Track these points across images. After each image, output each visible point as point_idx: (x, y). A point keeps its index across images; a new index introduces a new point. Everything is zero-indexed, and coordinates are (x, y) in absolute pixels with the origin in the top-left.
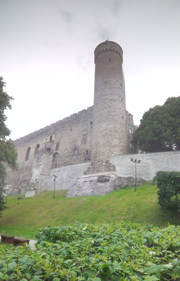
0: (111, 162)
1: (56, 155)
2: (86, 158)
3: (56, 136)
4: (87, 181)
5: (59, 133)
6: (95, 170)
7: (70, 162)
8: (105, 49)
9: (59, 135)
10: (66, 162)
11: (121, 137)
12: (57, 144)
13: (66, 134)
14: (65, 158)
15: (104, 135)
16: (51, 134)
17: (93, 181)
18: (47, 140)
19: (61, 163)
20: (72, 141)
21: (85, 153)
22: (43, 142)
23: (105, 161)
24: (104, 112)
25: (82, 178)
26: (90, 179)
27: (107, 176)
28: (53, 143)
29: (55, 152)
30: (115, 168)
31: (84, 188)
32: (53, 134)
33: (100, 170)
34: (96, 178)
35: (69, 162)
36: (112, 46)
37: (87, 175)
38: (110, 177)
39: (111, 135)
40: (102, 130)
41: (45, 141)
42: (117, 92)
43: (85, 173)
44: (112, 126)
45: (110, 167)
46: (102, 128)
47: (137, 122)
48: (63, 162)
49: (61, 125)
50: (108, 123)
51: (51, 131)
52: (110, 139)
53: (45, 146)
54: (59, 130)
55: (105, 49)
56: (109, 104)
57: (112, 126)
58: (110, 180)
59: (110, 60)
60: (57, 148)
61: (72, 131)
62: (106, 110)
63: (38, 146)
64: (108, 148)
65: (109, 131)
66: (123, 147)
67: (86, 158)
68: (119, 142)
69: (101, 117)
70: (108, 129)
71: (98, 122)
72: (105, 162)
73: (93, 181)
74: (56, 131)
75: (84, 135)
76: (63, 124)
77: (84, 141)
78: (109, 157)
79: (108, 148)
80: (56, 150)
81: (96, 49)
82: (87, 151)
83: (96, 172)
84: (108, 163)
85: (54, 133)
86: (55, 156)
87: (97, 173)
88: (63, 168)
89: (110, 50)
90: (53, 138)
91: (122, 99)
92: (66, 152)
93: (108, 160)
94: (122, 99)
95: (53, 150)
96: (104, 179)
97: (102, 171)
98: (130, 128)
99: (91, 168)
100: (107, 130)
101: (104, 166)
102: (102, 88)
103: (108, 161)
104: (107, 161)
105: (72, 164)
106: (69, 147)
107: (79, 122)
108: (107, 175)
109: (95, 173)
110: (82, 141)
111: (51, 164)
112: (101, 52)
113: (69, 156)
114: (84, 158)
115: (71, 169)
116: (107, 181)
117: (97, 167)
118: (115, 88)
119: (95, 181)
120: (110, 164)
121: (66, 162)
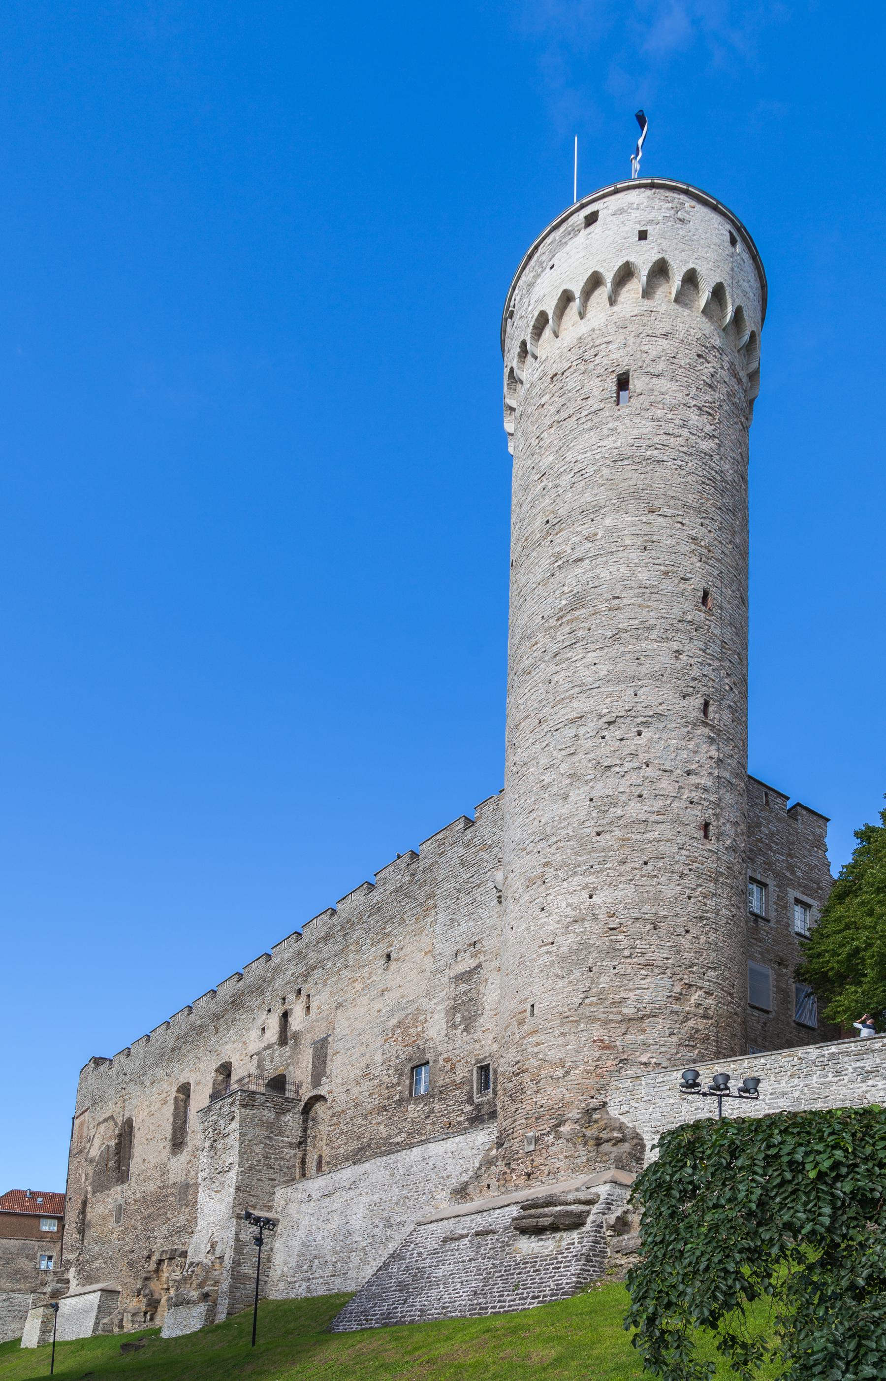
12: (316, 1050)
18: (268, 1033)
33: (546, 1169)
40: (553, 926)
46: (556, 917)
50: (592, 879)
60: (319, 1072)
62: (579, 795)
64: (597, 1031)
79: (597, 1031)
100: (587, 924)
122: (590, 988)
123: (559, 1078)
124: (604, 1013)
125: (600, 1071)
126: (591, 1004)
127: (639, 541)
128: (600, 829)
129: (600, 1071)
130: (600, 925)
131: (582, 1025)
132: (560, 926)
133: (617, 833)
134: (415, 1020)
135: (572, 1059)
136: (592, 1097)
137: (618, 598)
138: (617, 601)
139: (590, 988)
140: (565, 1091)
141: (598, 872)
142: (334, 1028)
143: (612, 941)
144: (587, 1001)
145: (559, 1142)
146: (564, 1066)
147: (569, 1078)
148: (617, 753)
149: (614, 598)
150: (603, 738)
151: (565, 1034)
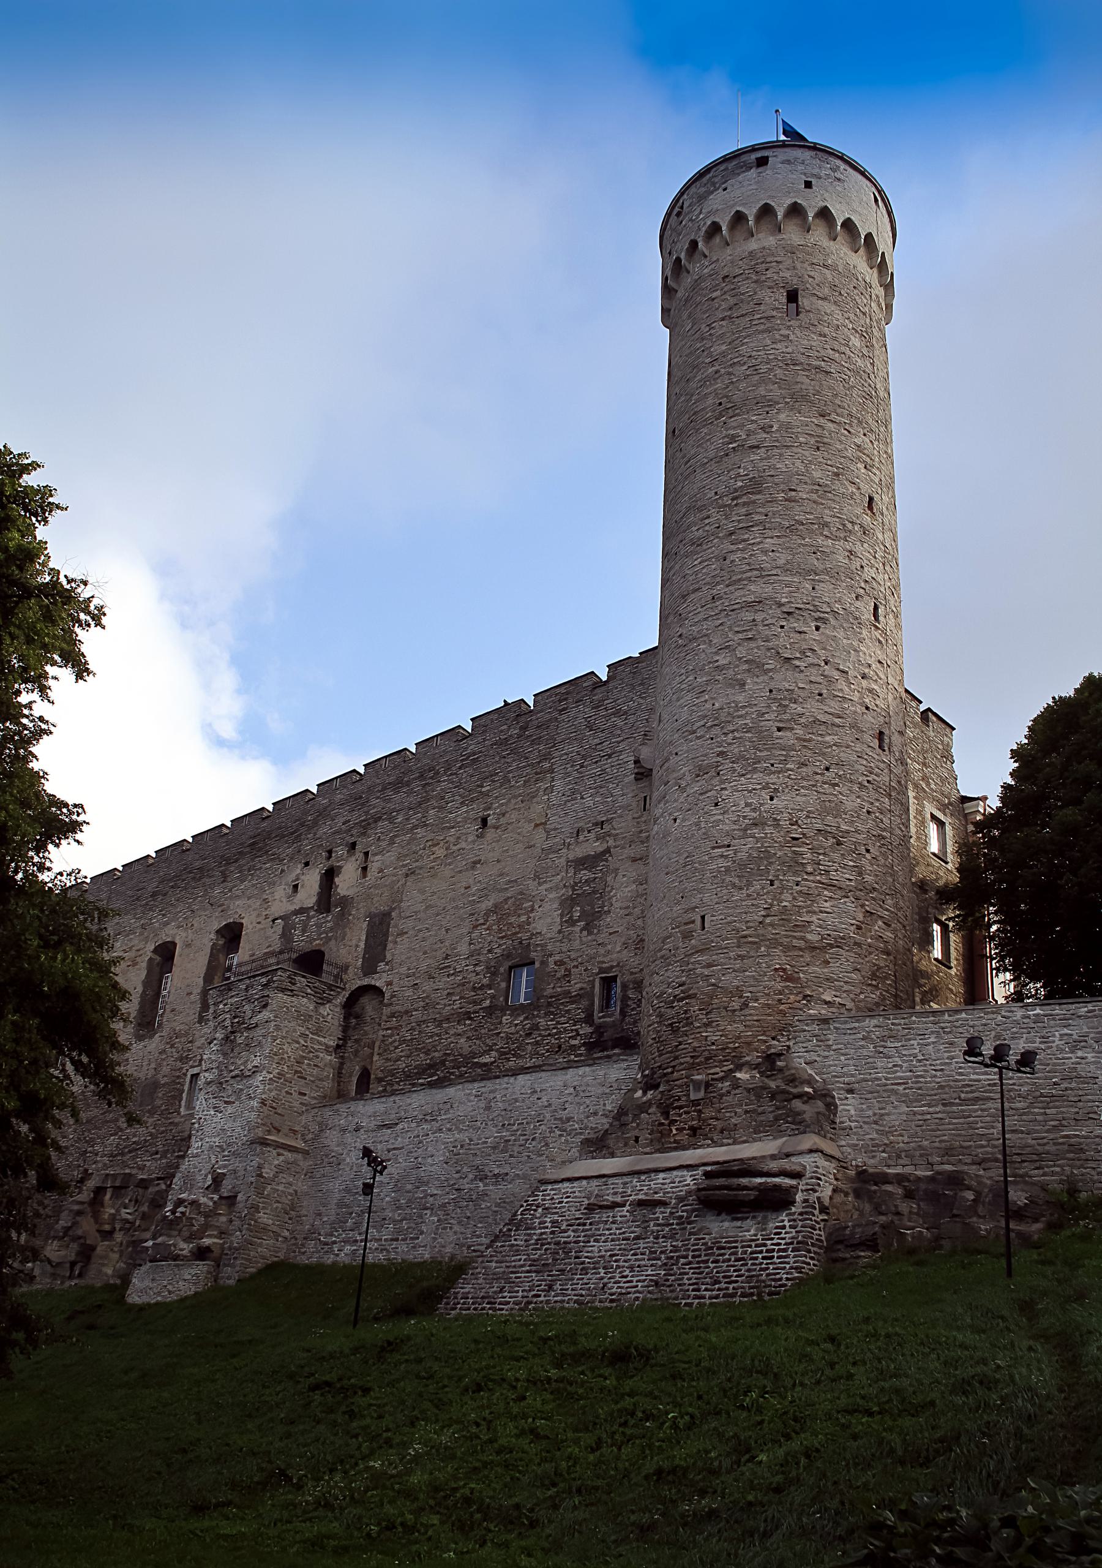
0: (799, 1061)
1: (368, 1004)
2: (599, 1030)
3: (365, 869)
4: (615, 1205)
5: (392, 842)
6: (673, 1122)
7: (474, 1055)
8: (751, 213)
9: (390, 857)
10: (443, 1062)
11: (868, 878)
13: (440, 852)
14: (431, 1028)
15: (743, 866)
16: (330, 852)
17: (663, 1203)
18: (301, 894)
19: (402, 1065)
20: (487, 904)
21: (591, 995)
22: (271, 904)
23: (753, 1057)
24: (741, 698)
25: (569, 1180)
26: (640, 1189)
27: (774, 1166)
28: (342, 915)
29: (355, 980)
30: (831, 1107)
31: (596, 1249)
32: (341, 851)
33: (719, 1124)
34: (689, 1180)
35: (468, 1060)
36: (808, 185)
37: (613, 1155)
38: (798, 1175)
39: (795, 865)
41: (280, 903)
42: (841, 558)
43: (597, 1145)
44: (809, 800)
45: (794, 1102)
47: (984, 772)
48: (423, 1059)
49: (408, 784)
50: (773, 778)
51: (324, 830)
52: (786, 896)
53: (286, 935)
54: (391, 820)
55: (751, 213)
56: (783, 641)
57: (809, 800)
58: (799, 1197)
59: (792, 296)
61: (490, 834)
63: (232, 935)
64: (779, 959)
65: (779, 837)
66: (888, 954)
67: (599, 1030)
68: (860, 917)
69: (716, 731)
70: (777, 824)
71: (700, 772)
72: (757, 1067)
73: (663, 1203)
74: (365, 827)
75: (581, 863)
76: (421, 777)
77: (585, 907)
78: (784, 1029)
79: (779, 959)
80: (369, 968)
81: (676, 210)
82: (608, 983)
83: (684, 1137)
84: (781, 1070)
85: (353, 846)
86: (357, 1009)
87: (695, 1147)
88: (419, 1101)
89: (796, 211)
90: (346, 883)
91: (876, 608)
92: (443, 982)
93: (776, 1046)
94: (876, 608)
95: (345, 968)
96: (746, 1188)
97: (729, 1135)
98: (933, 817)
99: (643, 1108)
101: (748, 1090)
102: (731, 527)
103: (779, 1055)
104: (770, 1059)
105: (487, 1073)
106: (463, 948)
107: (547, 765)
108: (773, 1157)
109: (680, 1147)
110: (567, 903)
111: (330, 1072)
112: (715, 228)
113: (468, 1016)
114: (586, 1029)
115: (488, 1108)
116: (775, 1200)
117: (696, 1103)
118: (826, 525)
119: (680, 1199)
120: (792, 1080)
121: (443, 1062)
122: (772, 905)
123: (735, 1011)
124: (787, 936)
125: (782, 1007)
126: (772, 925)
127: (812, 441)
128: (781, 725)
129: (782, 1007)
130: (782, 833)
131: (763, 949)
132: (737, 827)
133: (800, 732)
134: (519, 907)
135: (751, 989)
136: (773, 1039)
137: (794, 490)
138: (793, 493)
139: (772, 905)
140: (742, 1028)
141: (779, 772)
142: (401, 901)
143: (794, 852)
144: (768, 920)
145: (737, 1091)
146: (741, 997)
147: (746, 1012)
148: (796, 646)
149: (791, 490)
150: (782, 627)
151: (742, 957)
